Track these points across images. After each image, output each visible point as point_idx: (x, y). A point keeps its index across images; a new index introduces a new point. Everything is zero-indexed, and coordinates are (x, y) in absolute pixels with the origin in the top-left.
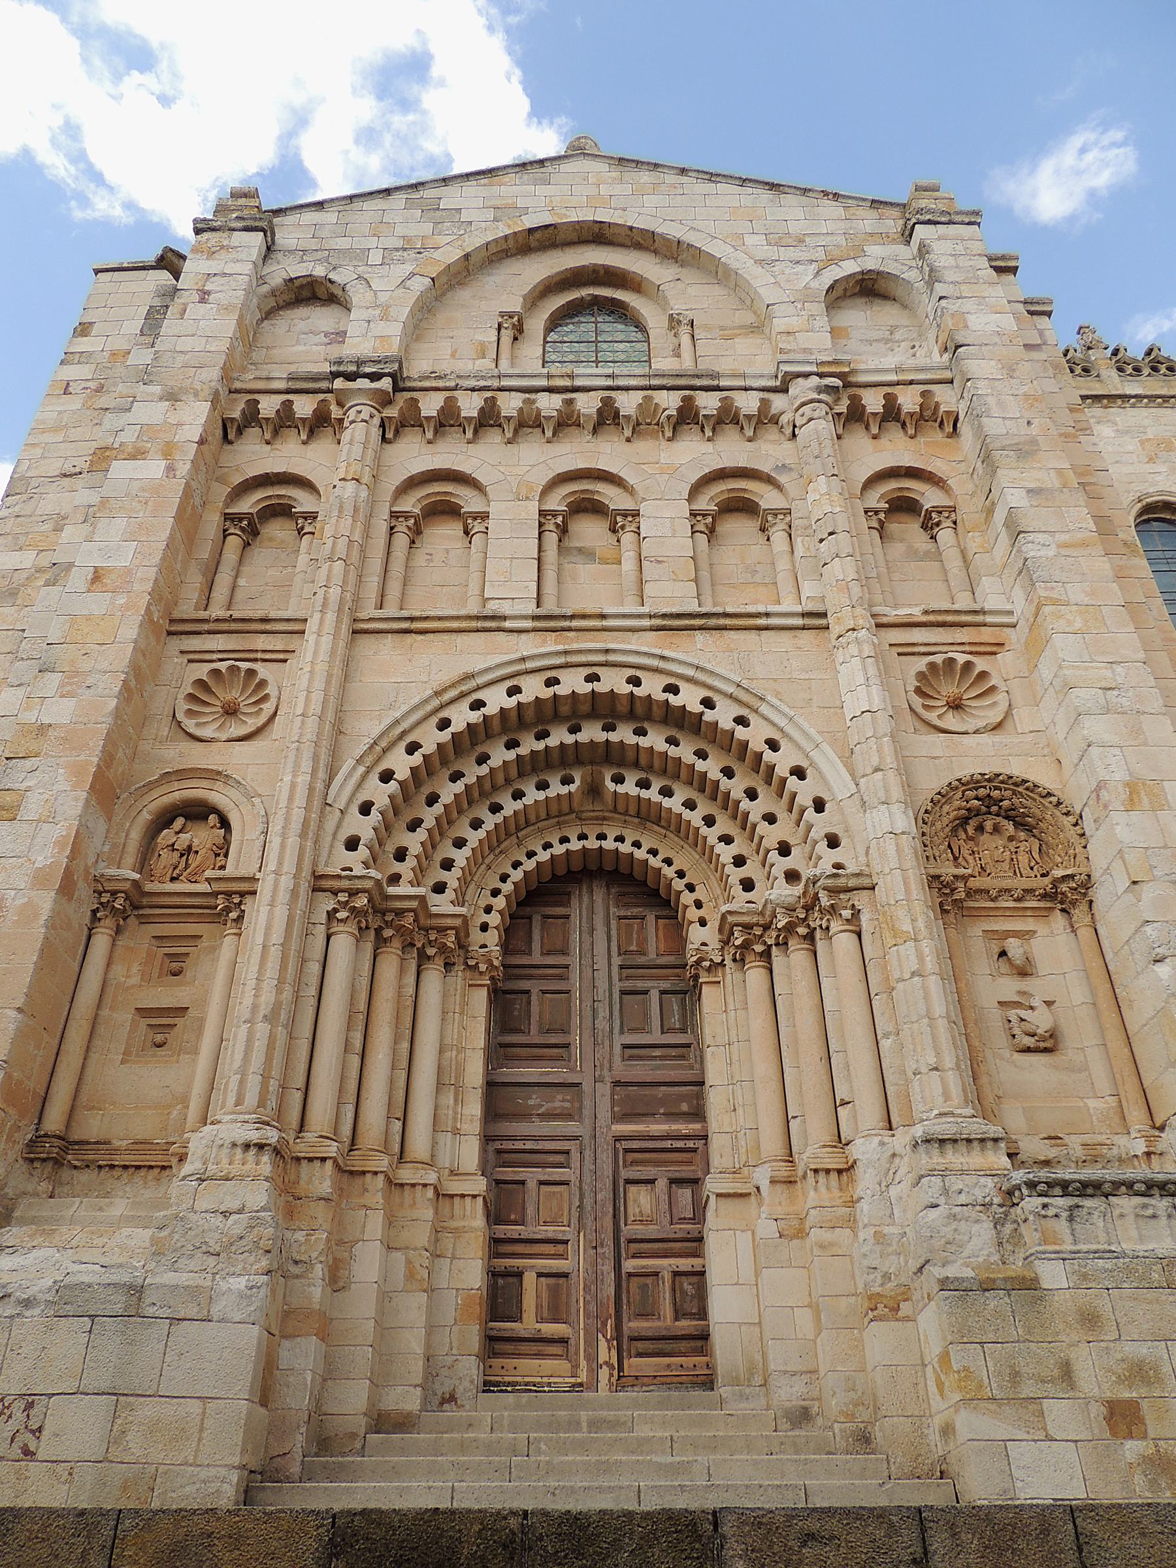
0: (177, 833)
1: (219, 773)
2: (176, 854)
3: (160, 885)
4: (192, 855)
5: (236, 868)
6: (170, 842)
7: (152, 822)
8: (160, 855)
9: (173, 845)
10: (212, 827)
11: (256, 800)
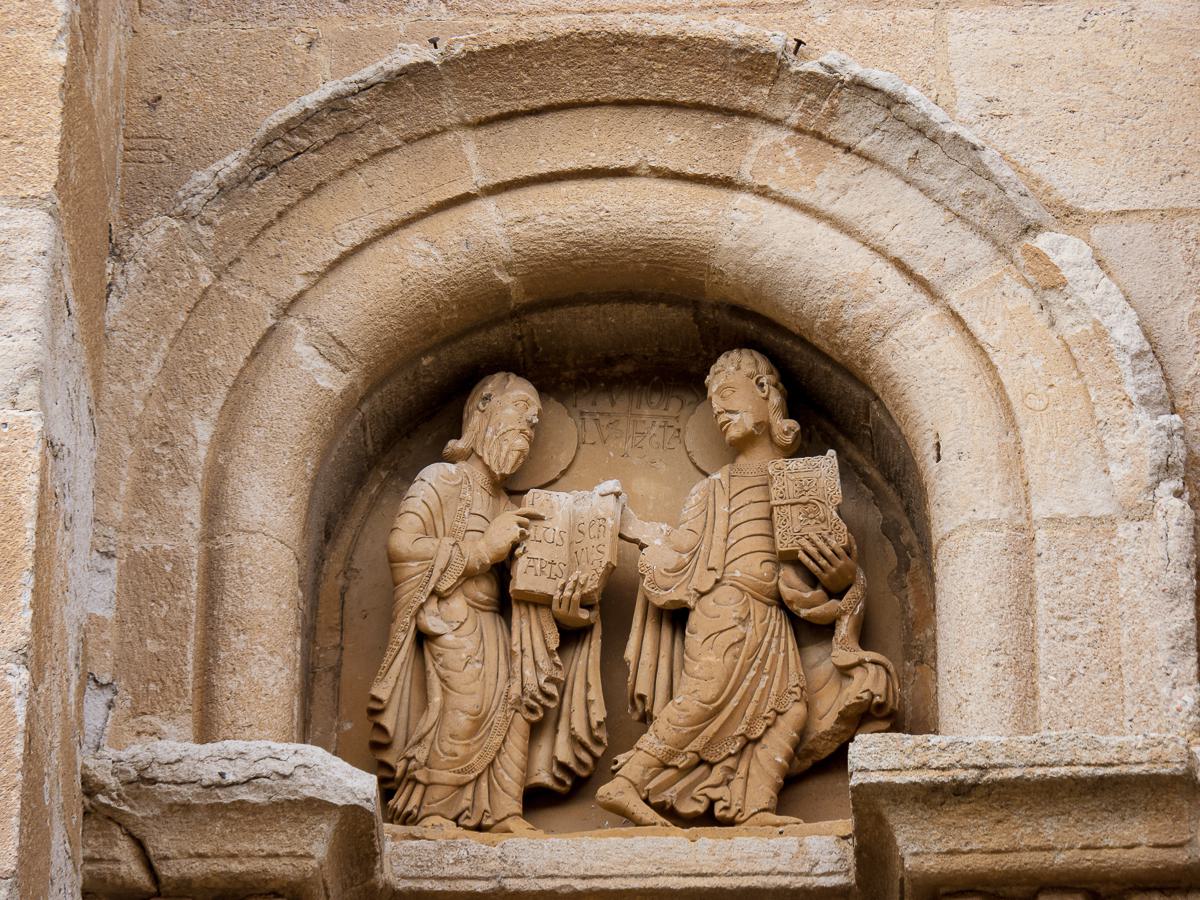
0: (508, 487)
1: (760, 65)
2: (533, 634)
3: (475, 843)
4: (642, 644)
5: (1025, 712)
6: (484, 549)
7: (349, 406)
8: (423, 639)
9: (501, 570)
10: (740, 447)
11: (1063, 248)
